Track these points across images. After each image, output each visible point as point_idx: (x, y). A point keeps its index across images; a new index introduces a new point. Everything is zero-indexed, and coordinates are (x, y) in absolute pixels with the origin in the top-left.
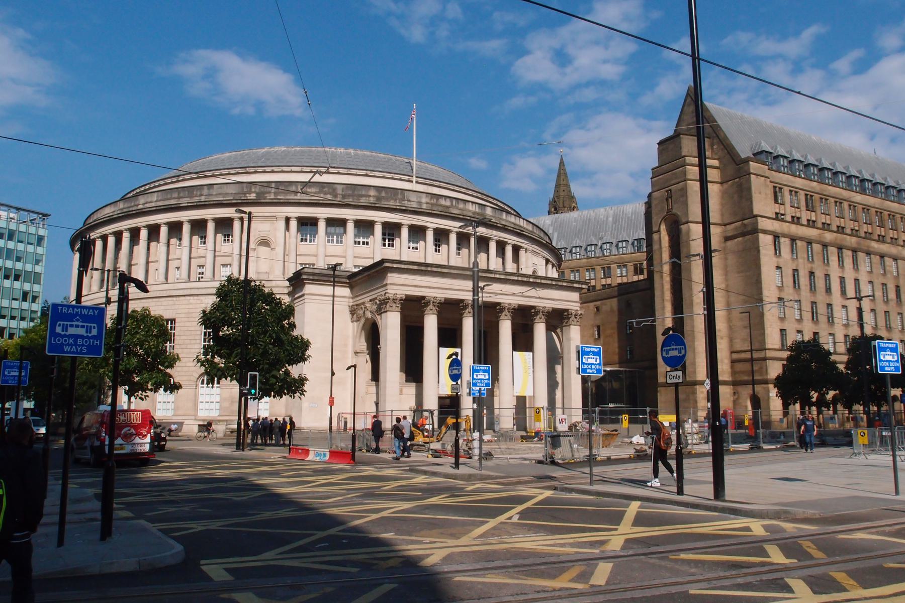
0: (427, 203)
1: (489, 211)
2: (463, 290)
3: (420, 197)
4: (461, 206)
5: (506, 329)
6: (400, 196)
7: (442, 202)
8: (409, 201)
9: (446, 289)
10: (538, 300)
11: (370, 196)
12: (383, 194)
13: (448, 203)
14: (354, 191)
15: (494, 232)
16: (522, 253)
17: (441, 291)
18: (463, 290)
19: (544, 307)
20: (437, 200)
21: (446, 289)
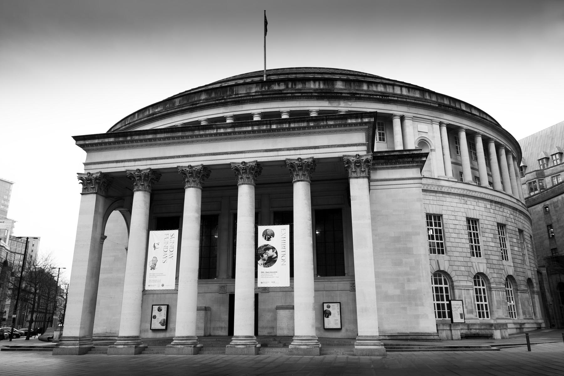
0: (256, 92)
1: (339, 85)
2: (179, 157)
3: (250, 88)
4: (299, 86)
5: (245, 196)
6: (228, 93)
7: (276, 87)
8: (238, 94)
9: (156, 159)
10: (292, 152)
11: (201, 100)
12: (213, 95)
13: (282, 87)
14: (188, 101)
15: (342, 104)
16: (397, 122)
17: (149, 162)
18: (179, 157)
19: (299, 159)
20: (269, 87)
21: (156, 159)
